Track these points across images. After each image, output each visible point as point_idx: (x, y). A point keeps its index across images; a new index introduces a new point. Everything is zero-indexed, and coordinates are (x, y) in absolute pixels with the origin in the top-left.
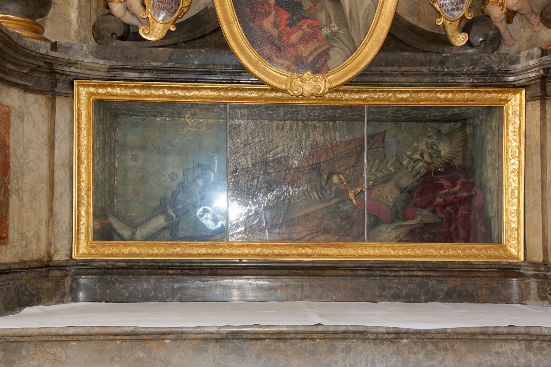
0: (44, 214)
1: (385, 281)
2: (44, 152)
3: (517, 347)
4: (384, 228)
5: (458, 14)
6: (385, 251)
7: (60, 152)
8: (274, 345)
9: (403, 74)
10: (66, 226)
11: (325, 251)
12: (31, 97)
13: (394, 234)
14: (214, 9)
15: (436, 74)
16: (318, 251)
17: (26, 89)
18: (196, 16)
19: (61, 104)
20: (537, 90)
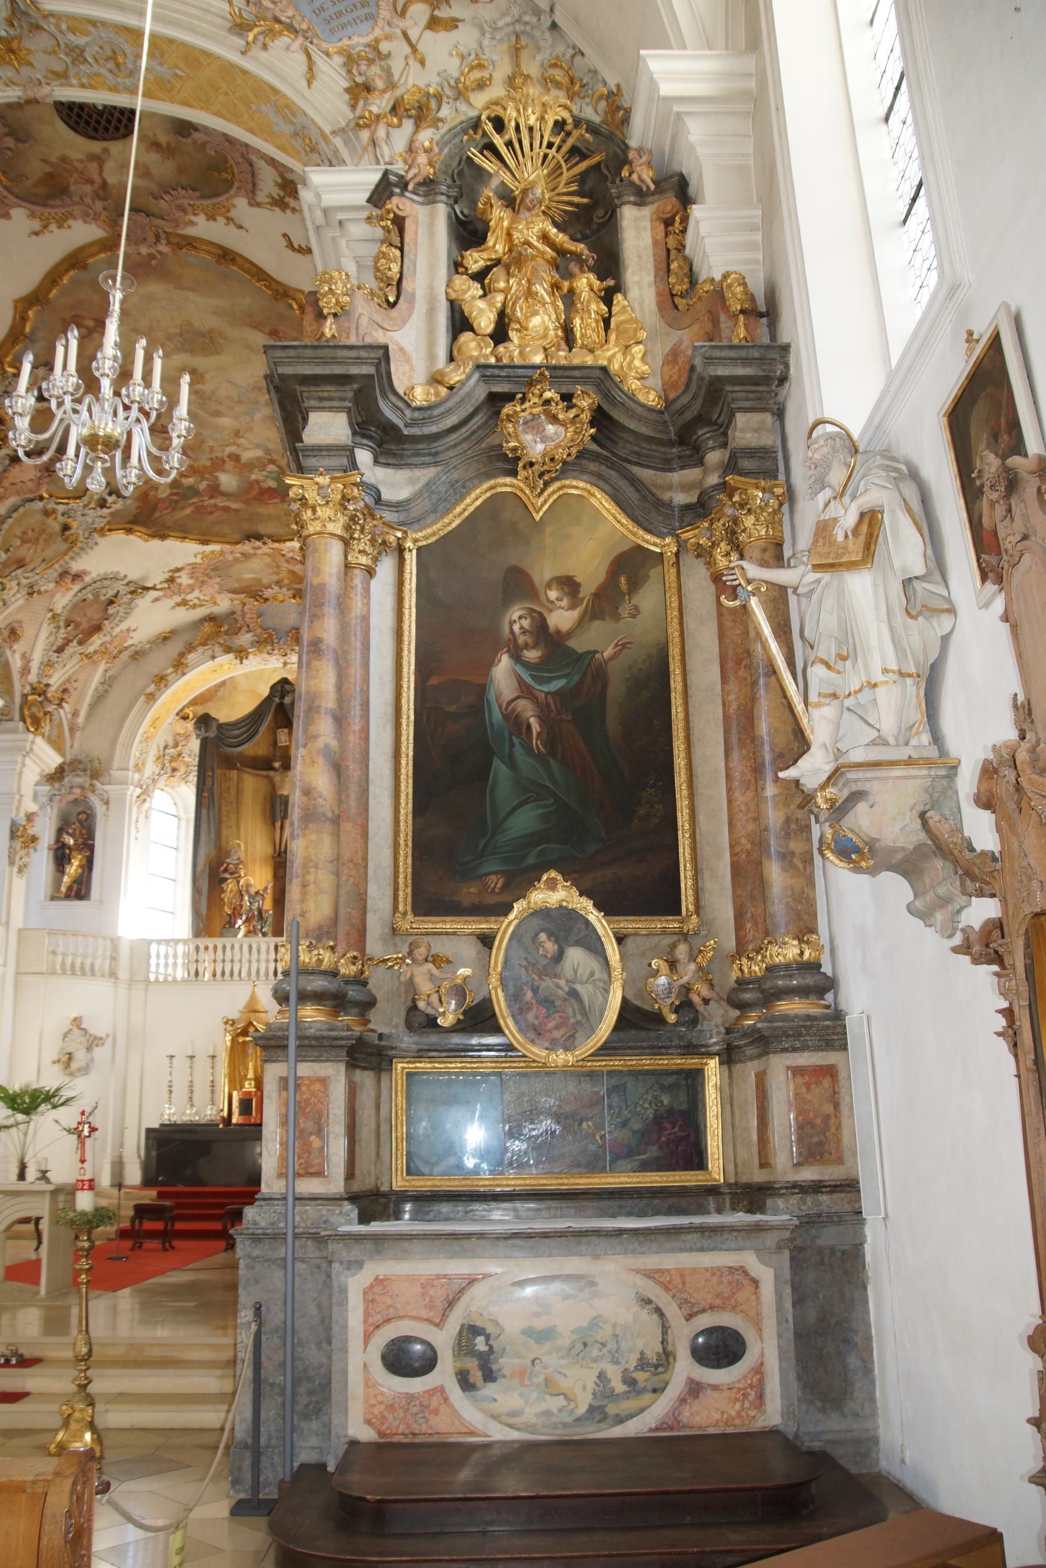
0: (373, 1157)
1: (623, 1203)
2: (373, 1112)
3: (695, 1236)
4: (621, 1162)
5: (669, 1001)
6: (623, 1179)
7: (384, 1112)
8: (542, 1240)
9: (630, 1048)
10: (387, 1165)
11: (578, 1181)
12: (366, 1073)
13: (629, 1167)
14: (490, 1000)
15: (654, 1047)
16: (572, 1181)
17: (364, 1068)
18: (478, 1005)
19: (384, 1076)
20: (725, 1057)
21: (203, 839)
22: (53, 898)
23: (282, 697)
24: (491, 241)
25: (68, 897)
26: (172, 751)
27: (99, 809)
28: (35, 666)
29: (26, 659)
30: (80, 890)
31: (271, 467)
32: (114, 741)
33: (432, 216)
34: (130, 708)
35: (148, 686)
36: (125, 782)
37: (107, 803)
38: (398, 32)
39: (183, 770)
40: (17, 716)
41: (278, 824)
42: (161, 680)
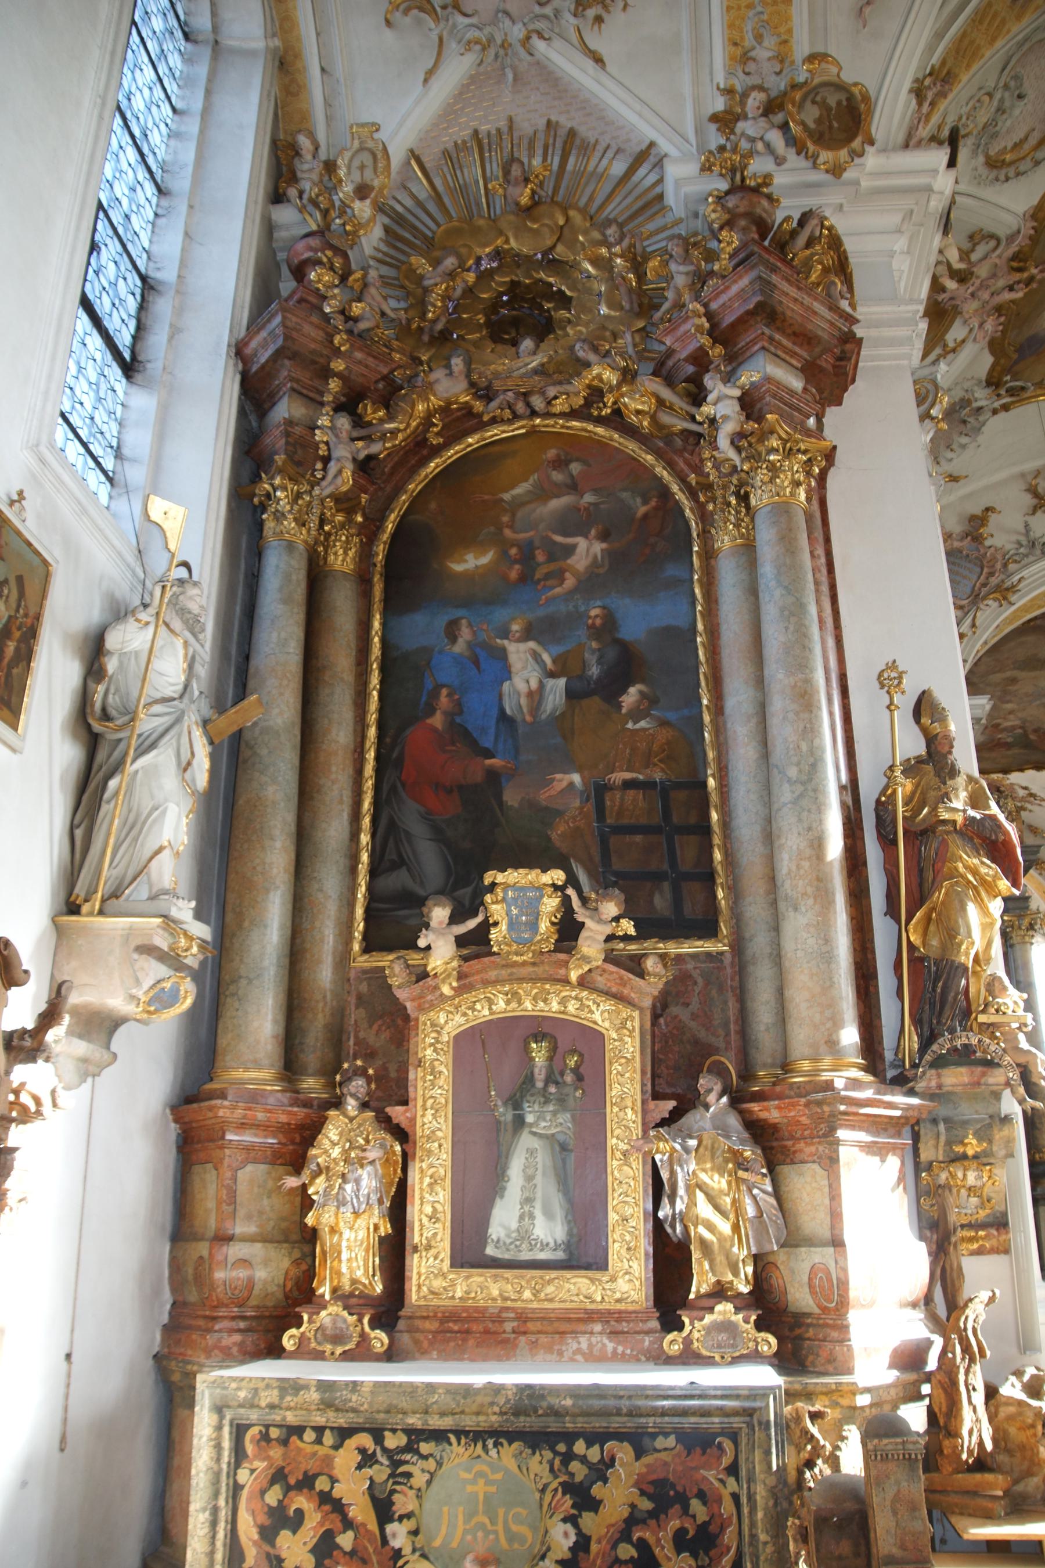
31: (1020, 731)
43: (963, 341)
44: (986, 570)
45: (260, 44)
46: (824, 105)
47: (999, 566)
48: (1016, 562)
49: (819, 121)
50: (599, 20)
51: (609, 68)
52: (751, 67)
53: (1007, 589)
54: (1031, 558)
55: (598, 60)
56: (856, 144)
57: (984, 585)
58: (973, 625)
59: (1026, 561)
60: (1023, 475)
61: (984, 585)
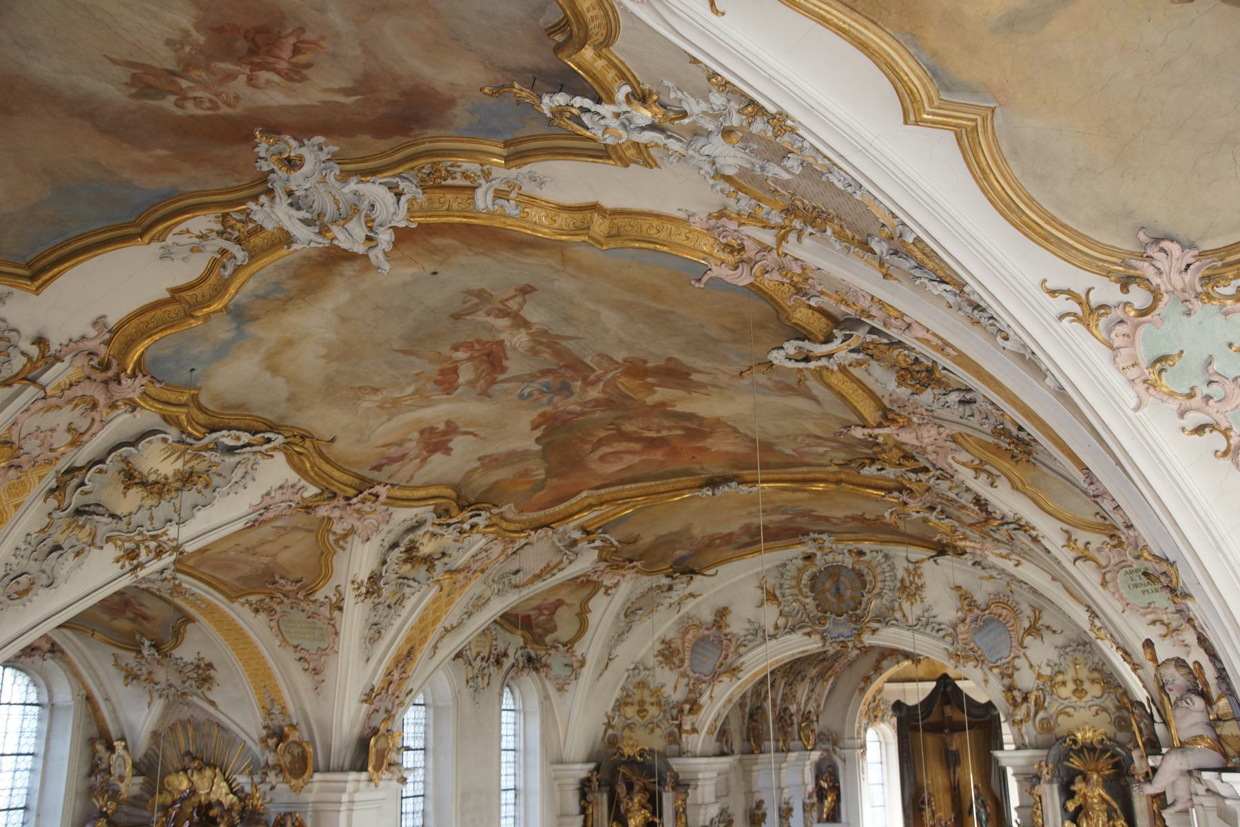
21: (907, 784)
22: (819, 822)
23: (945, 687)
24: (1076, 797)
25: (828, 820)
26: (872, 705)
27: (840, 764)
28: (802, 706)
29: (799, 704)
30: (834, 816)
32: (843, 720)
33: (1052, 789)
34: (851, 697)
35: (859, 684)
36: (853, 748)
37: (844, 761)
38: (1021, 653)
39: (880, 715)
40: (797, 737)
41: (952, 770)
42: (868, 680)
43: (618, 583)
44: (724, 652)
45: (73, 703)
46: (292, 754)
47: (732, 649)
48: (745, 646)
49: (290, 763)
50: (209, 689)
51: (221, 708)
52: (272, 716)
53: (734, 669)
54: (755, 643)
55: (212, 703)
56: (306, 776)
57: (721, 664)
58: (711, 697)
59: (751, 645)
60: (758, 574)
61: (721, 664)
